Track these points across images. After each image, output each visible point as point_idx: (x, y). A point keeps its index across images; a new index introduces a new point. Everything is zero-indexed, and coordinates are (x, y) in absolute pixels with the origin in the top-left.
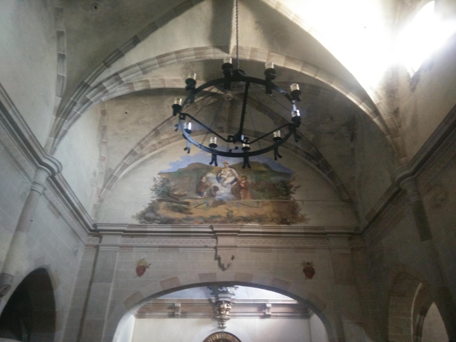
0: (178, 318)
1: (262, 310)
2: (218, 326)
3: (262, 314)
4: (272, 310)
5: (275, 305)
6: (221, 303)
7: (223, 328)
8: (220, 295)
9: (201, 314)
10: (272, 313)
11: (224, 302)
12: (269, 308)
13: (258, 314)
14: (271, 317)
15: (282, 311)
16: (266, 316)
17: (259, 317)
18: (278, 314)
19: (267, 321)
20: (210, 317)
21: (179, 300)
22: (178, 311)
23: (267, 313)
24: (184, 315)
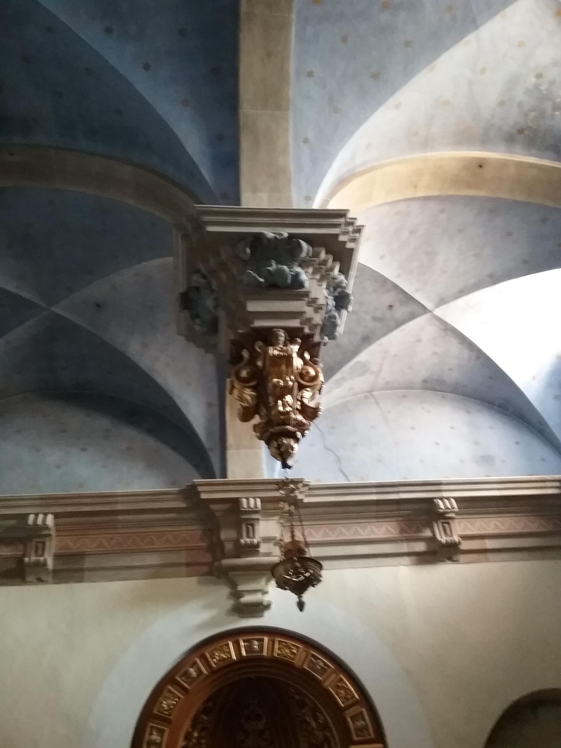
0: (40, 581)
1: (419, 531)
2: (231, 603)
3: (420, 547)
4: (460, 528)
5: (473, 506)
6: (268, 337)
7: (259, 608)
8: (253, 306)
9: (153, 559)
10: (465, 538)
11: (282, 335)
12: (443, 518)
13: (404, 548)
14: (462, 557)
15: (504, 530)
16: (441, 553)
17: (406, 560)
18: (490, 544)
19: (445, 573)
20: (191, 567)
21: (47, 502)
22: (41, 549)
23: (443, 539)
24: (70, 569)
